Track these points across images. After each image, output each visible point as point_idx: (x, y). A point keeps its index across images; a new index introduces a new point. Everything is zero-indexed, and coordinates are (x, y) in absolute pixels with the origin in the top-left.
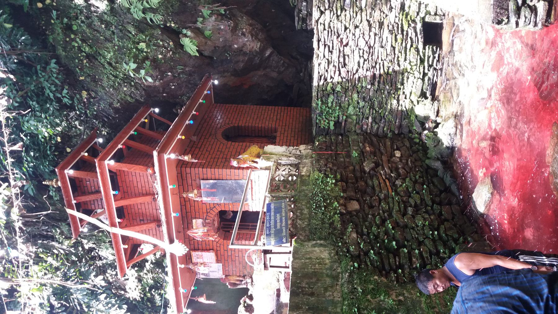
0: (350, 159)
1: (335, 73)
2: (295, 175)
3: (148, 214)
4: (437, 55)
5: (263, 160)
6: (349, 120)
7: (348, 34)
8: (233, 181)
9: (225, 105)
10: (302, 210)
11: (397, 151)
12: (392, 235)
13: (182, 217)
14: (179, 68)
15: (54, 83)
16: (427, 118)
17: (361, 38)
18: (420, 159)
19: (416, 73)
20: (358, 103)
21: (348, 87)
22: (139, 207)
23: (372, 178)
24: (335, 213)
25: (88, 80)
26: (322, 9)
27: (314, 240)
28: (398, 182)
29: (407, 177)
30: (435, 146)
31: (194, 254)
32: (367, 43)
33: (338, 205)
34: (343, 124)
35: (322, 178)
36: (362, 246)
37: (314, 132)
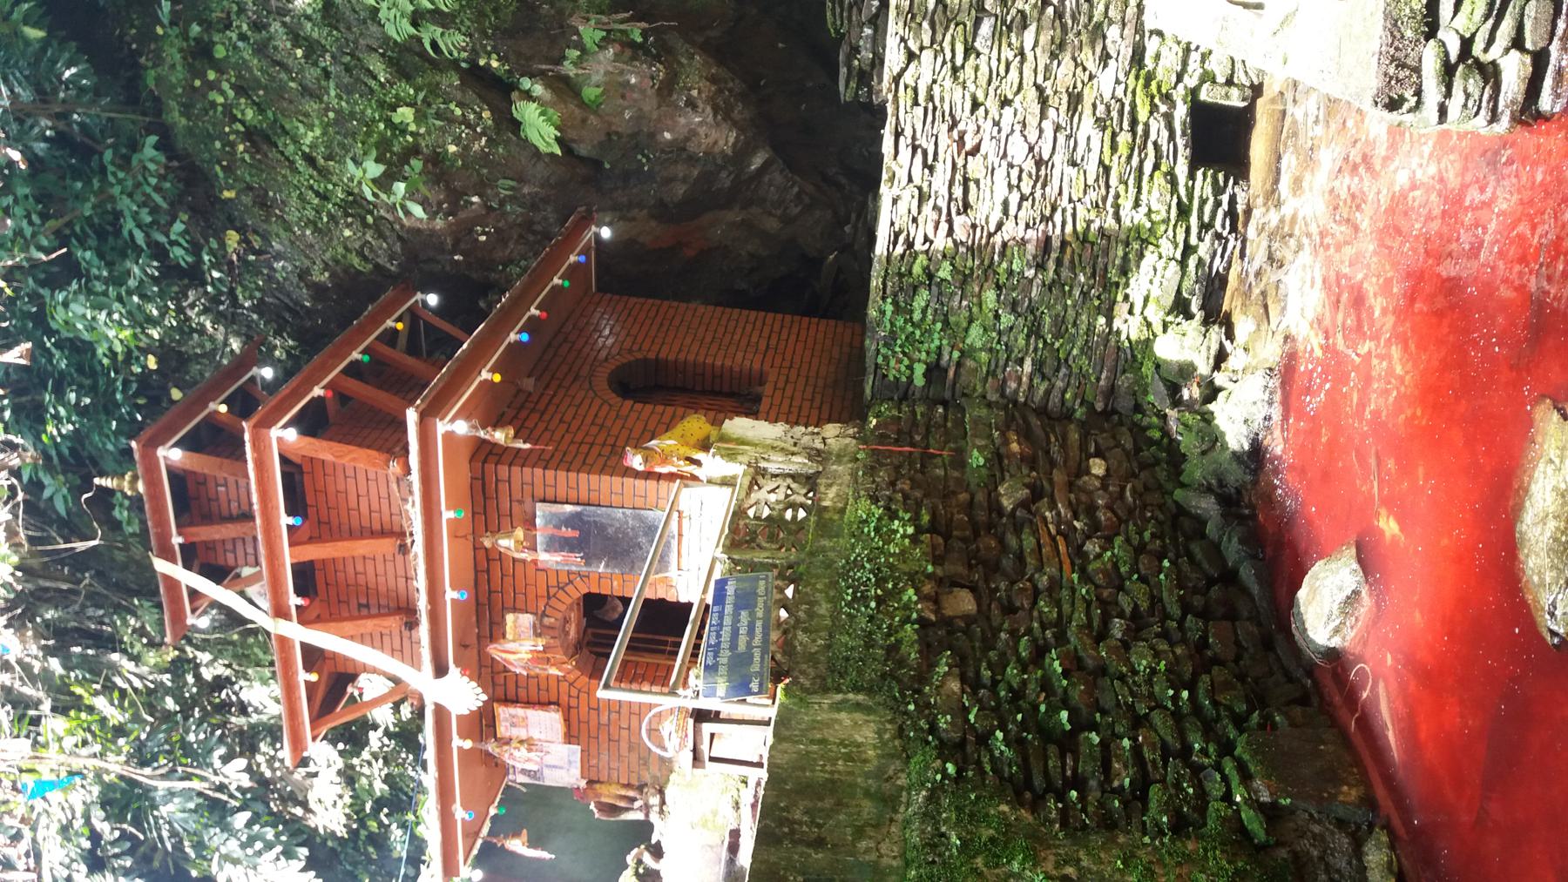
0: (963, 473)
1: (936, 228)
2: (802, 506)
3: (382, 589)
4: (1225, 198)
5: (718, 457)
6: (970, 363)
7: (981, 121)
8: (628, 512)
9: (625, 298)
10: (812, 604)
11: (1097, 460)
12: (1060, 691)
13: (478, 604)
14: (504, 187)
15: (146, 202)
16: (1186, 371)
17: (1017, 133)
18: (1160, 487)
19: (1164, 242)
20: (997, 317)
21: (972, 269)
22: (360, 568)
23: (1018, 531)
24: (907, 620)
25: (247, 199)
26: (914, 47)
27: (839, 690)
28: (1092, 547)
29: (1118, 534)
30: (1204, 453)
31: (503, 712)
32: (1031, 149)
33: (915, 598)
34: (951, 373)
35: (880, 519)
36: (972, 717)
37: (868, 391)
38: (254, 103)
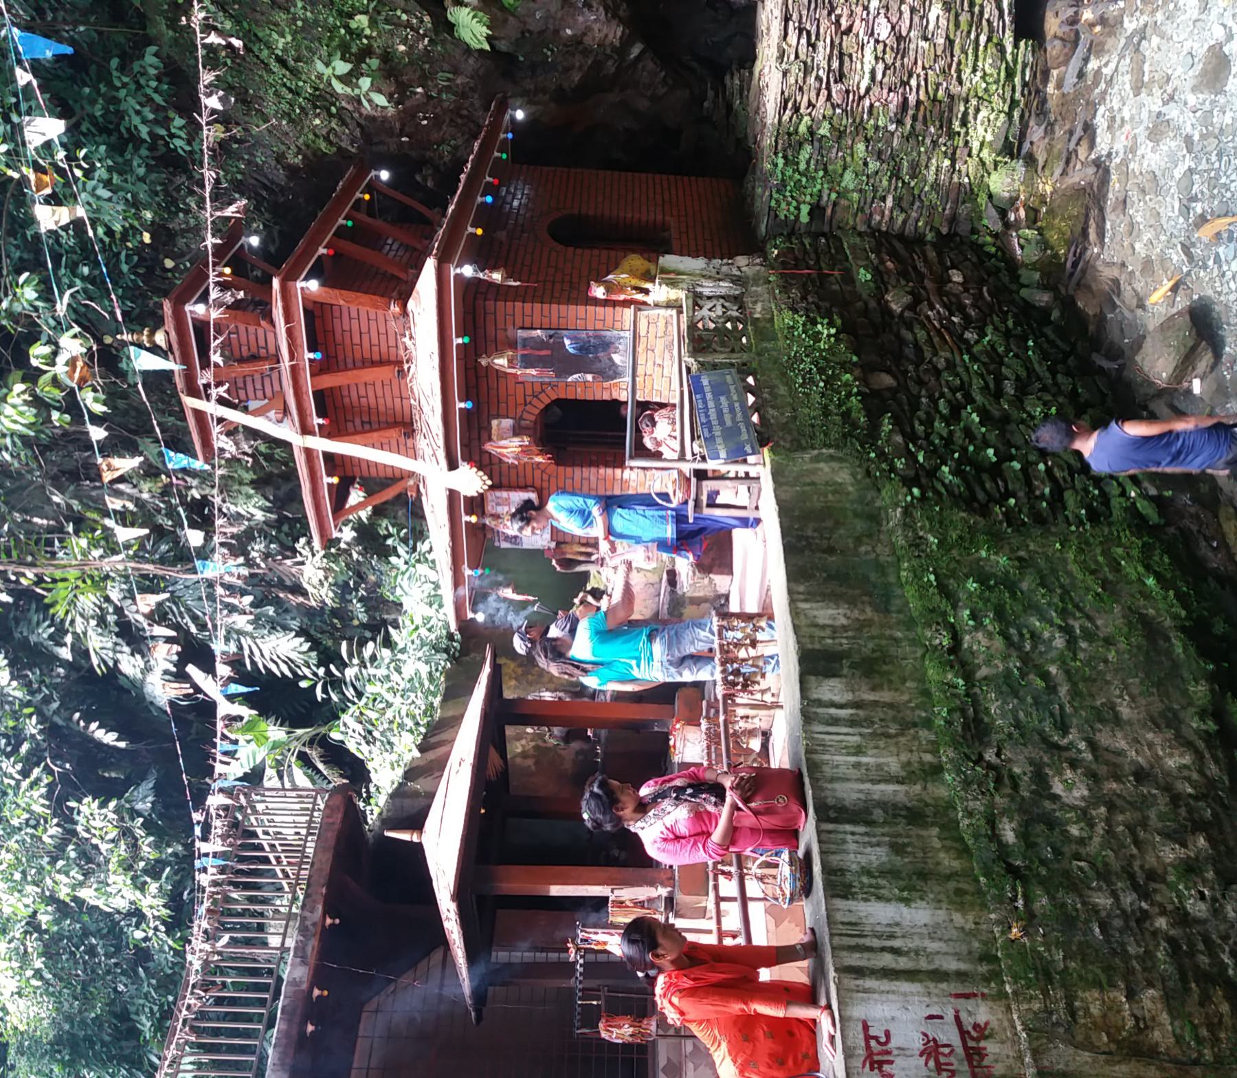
2: (738, 319)
6: (843, 202)
10: (772, 387)
14: (442, 79)
19: (995, 98)
20: (866, 164)
24: (849, 395)
28: (970, 336)
29: (985, 325)
34: (829, 211)
36: (921, 459)
38: (231, 16)
